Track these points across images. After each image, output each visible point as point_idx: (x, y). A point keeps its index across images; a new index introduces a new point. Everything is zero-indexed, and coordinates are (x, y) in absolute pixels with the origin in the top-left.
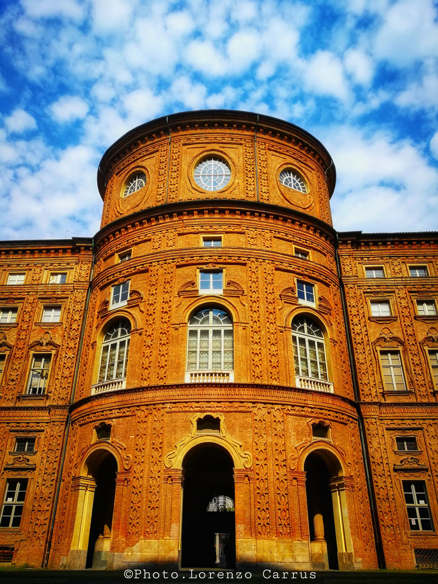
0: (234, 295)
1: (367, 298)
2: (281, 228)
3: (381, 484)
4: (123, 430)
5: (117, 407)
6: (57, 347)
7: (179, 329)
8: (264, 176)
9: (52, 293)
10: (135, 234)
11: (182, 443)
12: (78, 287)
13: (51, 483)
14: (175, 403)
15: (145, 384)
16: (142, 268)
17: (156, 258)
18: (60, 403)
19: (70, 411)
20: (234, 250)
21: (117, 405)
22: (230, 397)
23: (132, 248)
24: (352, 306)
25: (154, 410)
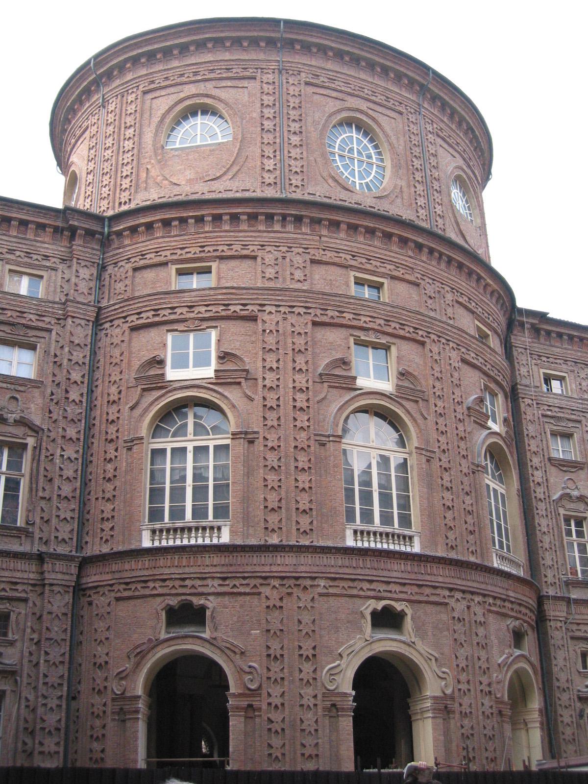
0: (410, 397)
1: (547, 426)
2: (466, 288)
3: (567, 719)
4: (235, 619)
5: (219, 575)
6: (37, 433)
7: (328, 445)
8: (436, 185)
9: (18, 314)
10: (220, 237)
11: (350, 650)
12: (75, 312)
13: (58, 702)
14: (335, 579)
15: (274, 540)
16: (241, 310)
17: (273, 297)
18: (61, 550)
19: (80, 568)
20: (410, 314)
21: (219, 570)
22: (420, 577)
23: (214, 265)
24: (530, 435)
25: (295, 590)
